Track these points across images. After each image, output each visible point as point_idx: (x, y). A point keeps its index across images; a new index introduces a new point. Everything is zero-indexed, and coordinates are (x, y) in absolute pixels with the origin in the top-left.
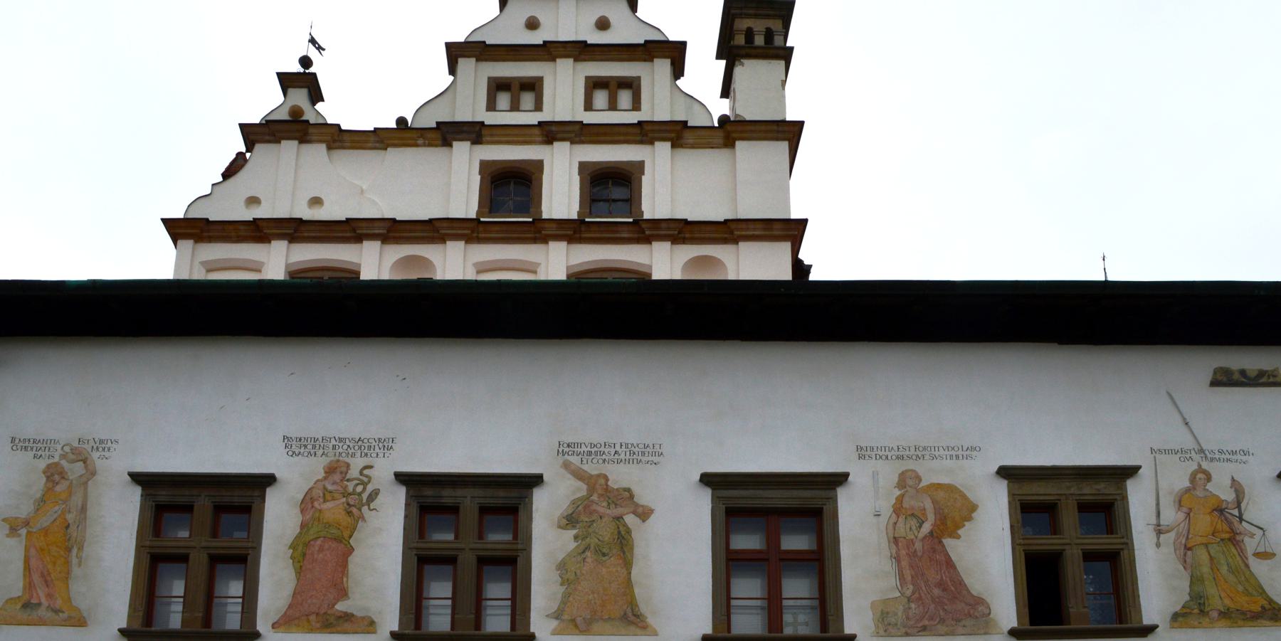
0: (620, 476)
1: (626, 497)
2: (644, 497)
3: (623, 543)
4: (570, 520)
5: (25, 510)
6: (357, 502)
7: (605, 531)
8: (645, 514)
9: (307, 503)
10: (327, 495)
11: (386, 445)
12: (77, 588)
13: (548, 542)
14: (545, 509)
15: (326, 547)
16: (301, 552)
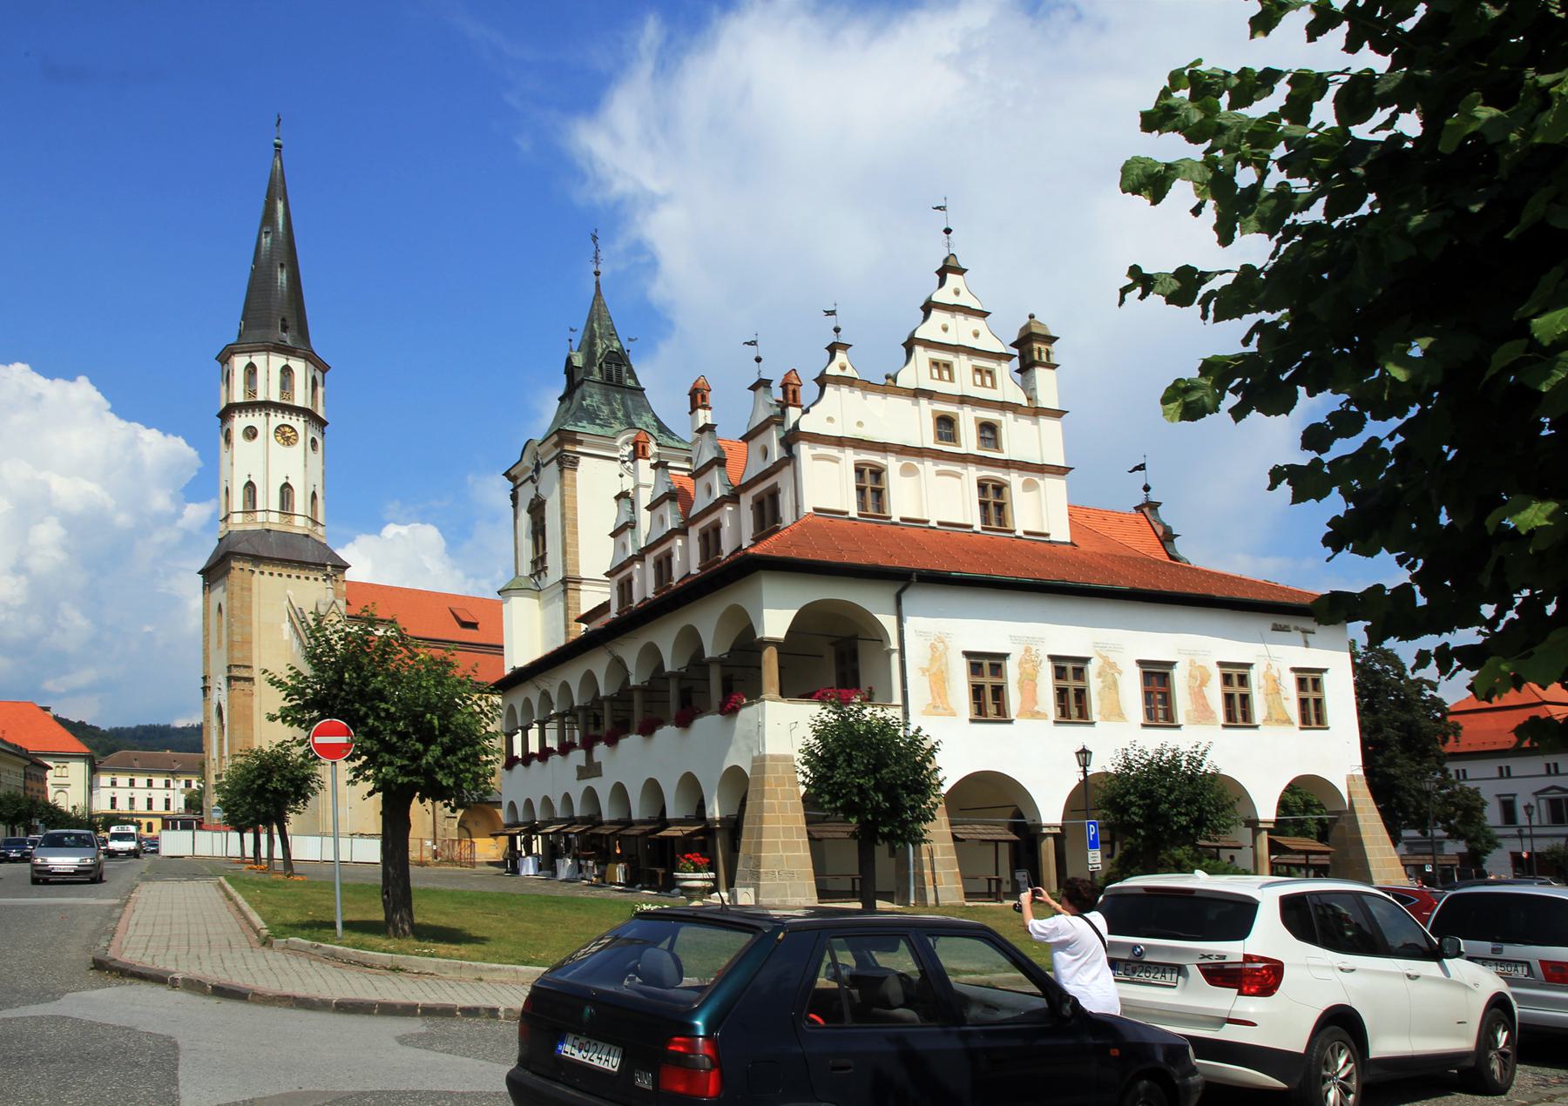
0: (1113, 657)
1: (1113, 666)
2: (1120, 667)
3: (1115, 683)
4: (1100, 675)
5: (926, 666)
6: (1036, 668)
7: (1109, 679)
8: (1120, 673)
9: (1020, 665)
10: (1027, 662)
11: (1042, 640)
12: (950, 699)
13: (1094, 683)
14: (1092, 670)
15: (1028, 683)
16: (1021, 683)
